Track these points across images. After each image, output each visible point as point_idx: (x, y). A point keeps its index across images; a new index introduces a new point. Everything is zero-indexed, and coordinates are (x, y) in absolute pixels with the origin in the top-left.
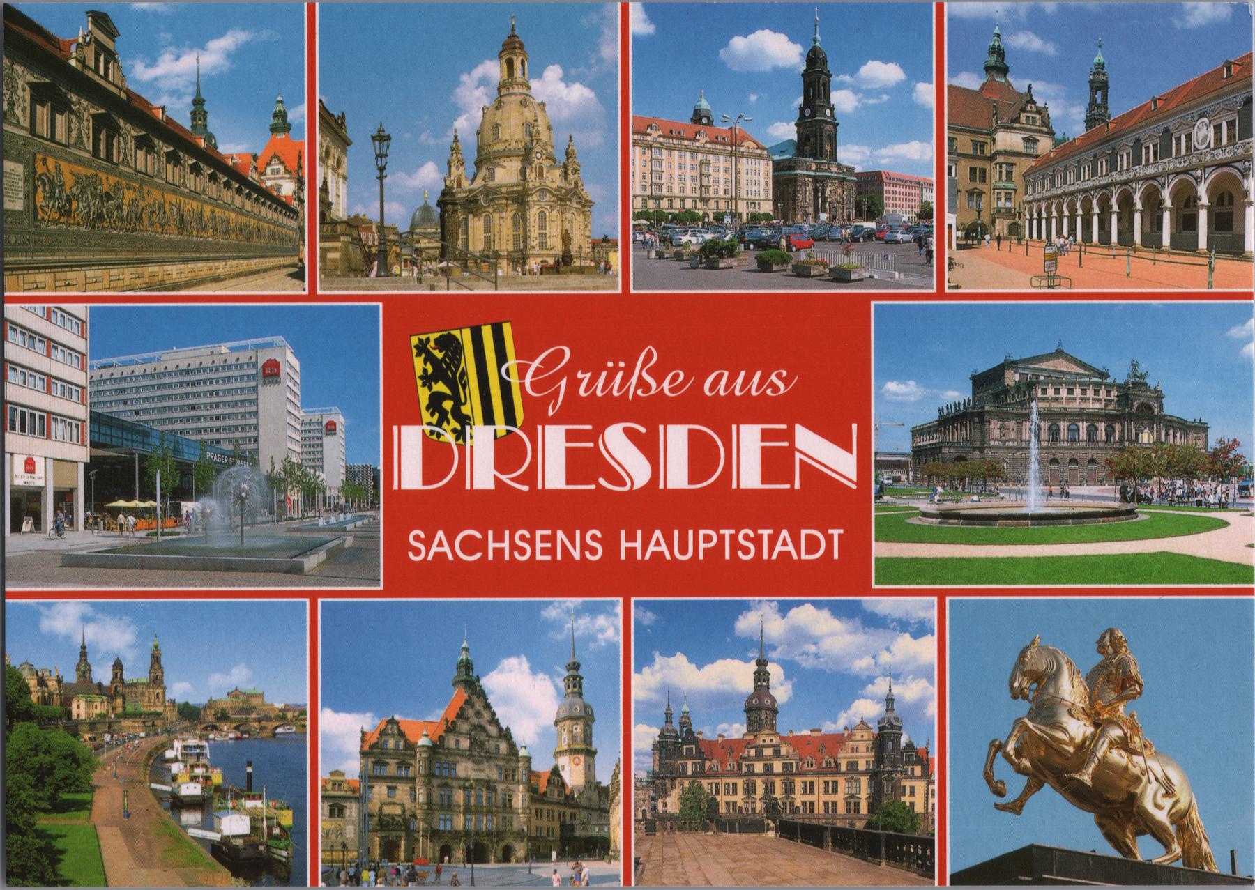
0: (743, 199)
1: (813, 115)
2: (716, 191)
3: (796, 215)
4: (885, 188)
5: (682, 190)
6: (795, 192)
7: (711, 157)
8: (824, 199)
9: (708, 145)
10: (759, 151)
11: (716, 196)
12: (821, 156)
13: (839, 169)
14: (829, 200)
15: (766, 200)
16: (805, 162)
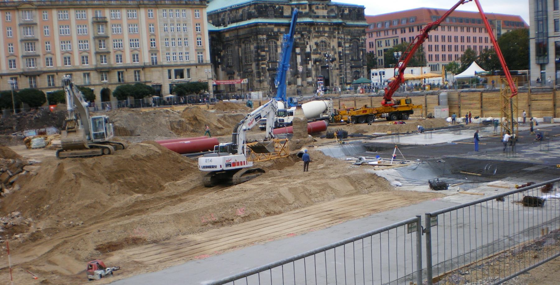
2: (119, 58)
5: (67, 60)
11: (120, 64)
14: (313, 57)
15: (201, 63)
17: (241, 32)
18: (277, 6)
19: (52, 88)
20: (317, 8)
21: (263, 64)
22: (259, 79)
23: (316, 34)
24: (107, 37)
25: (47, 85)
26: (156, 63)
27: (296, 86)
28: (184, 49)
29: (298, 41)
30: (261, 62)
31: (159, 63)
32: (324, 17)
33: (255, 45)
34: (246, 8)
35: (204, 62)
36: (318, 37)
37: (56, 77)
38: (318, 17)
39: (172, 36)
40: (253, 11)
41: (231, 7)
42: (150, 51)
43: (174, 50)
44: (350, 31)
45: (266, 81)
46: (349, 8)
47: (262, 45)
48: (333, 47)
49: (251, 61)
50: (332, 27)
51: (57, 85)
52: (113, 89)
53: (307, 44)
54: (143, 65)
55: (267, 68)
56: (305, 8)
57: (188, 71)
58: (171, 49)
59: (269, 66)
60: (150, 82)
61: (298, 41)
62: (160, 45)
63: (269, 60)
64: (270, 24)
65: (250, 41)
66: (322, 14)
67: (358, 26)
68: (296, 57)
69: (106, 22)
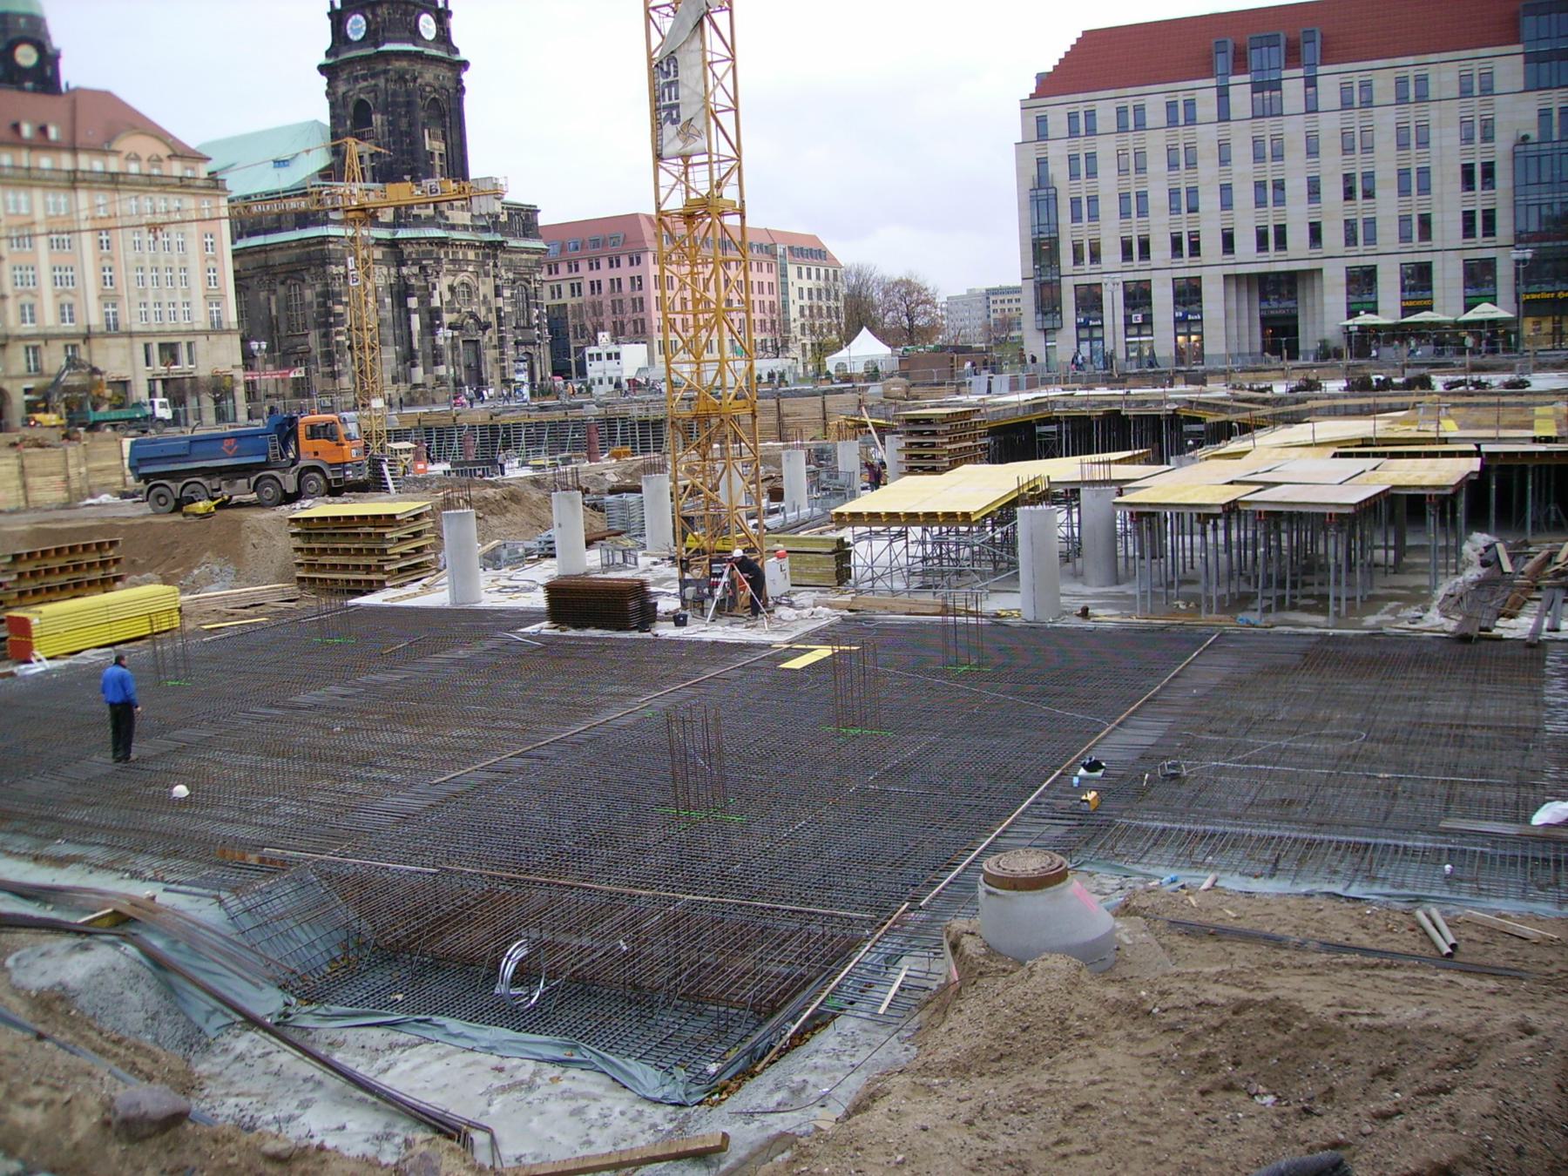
1: (372, 37)
10: (176, 168)
14: (447, 318)
17: (277, 258)
20: (452, 207)
21: (339, 333)
23: (451, 267)
26: (116, 326)
28: (179, 292)
29: (413, 281)
30: (334, 330)
31: (122, 328)
32: (465, 227)
33: (319, 288)
35: (225, 326)
36: (454, 273)
38: (453, 227)
39: (153, 261)
42: (100, 298)
43: (157, 295)
44: (511, 260)
47: (337, 289)
48: (485, 297)
49: (305, 326)
50: (480, 252)
53: (434, 288)
54: (83, 330)
55: (348, 343)
58: (151, 294)
62: (126, 282)
65: (304, 281)
66: (460, 222)
67: (527, 251)
68: (409, 319)
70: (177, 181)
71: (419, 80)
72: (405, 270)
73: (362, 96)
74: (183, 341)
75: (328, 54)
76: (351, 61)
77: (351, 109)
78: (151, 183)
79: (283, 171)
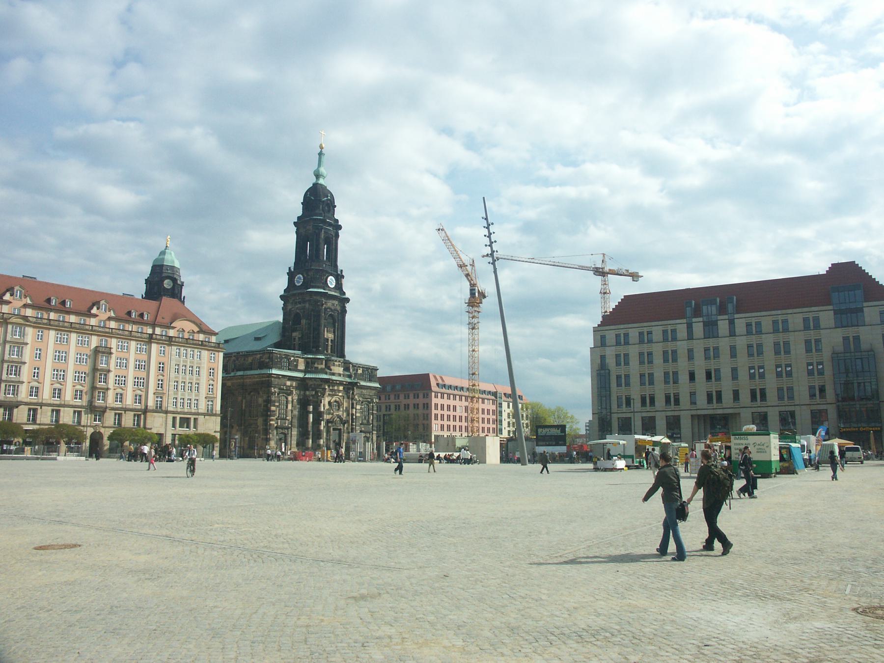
0: (167, 412)
1: (306, 285)
3: (267, 440)
4: (434, 401)
5: (58, 393)
6: (268, 402)
7: (114, 343)
8: (318, 416)
9: (113, 324)
10: (201, 337)
11: (118, 405)
12: (317, 347)
13: (346, 369)
14: (327, 417)
15: (210, 413)
16: (287, 356)
18: (292, 358)
19: (31, 424)
20: (334, 365)
21: (272, 420)
22: (265, 437)
23: (331, 393)
24: (109, 371)
25: (25, 420)
26: (161, 407)
27: (304, 448)
32: (340, 375)
33: (265, 397)
34: (259, 356)
35: (214, 412)
36: (332, 396)
37: (39, 411)
38: (333, 374)
40: (267, 360)
41: (238, 353)
42: (154, 394)
43: (182, 395)
45: (274, 439)
46: (362, 367)
51: (38, 422)
52: (107, 433)
55: (276, 425)
56: (322, 364)
57: (195, 419)
58: (180, 393)
59: (277, 423)
60: (151, 429)
61: (311, 398)
63: (279, 416)
64: (284, 376)
65: (259, 394)
69: (111, 353)
70: (200, 343)
71: (324, 305)
72: (308, 393)
73: (298, 311)
74: (192, 417)
75: (285, 291)
76: (294, 295)
77: (292, 316)
78: (188, 343)
79: (258, 342)
